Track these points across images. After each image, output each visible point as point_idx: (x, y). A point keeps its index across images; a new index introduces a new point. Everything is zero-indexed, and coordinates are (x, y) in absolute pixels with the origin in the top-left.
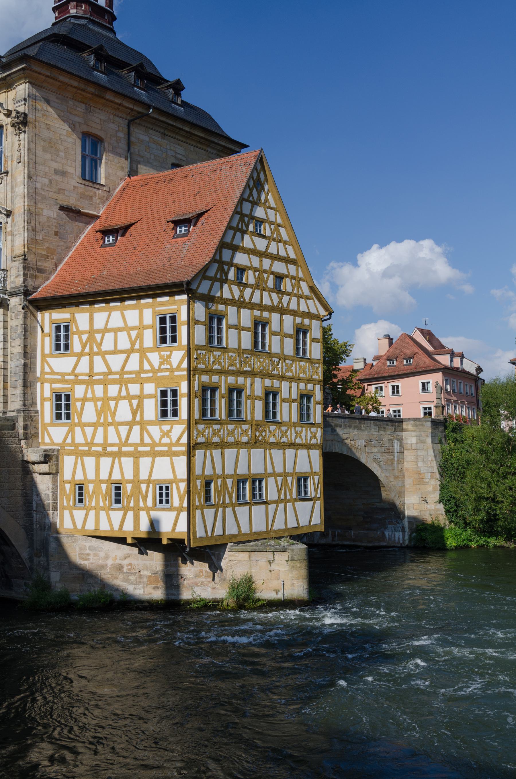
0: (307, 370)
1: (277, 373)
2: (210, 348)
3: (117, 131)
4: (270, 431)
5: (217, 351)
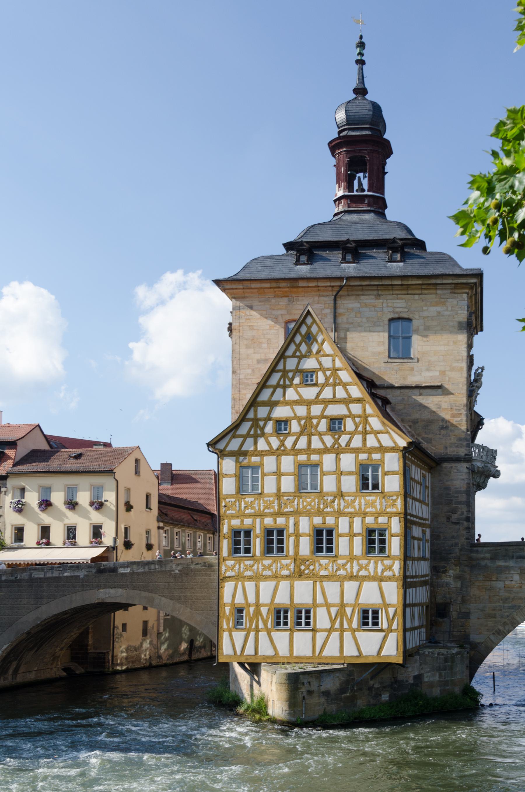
0: (378, 503)
1: (332, 510)
2: (241, 496)
3: (322, 310)
4: (320, 565)
5: (249, 497)
